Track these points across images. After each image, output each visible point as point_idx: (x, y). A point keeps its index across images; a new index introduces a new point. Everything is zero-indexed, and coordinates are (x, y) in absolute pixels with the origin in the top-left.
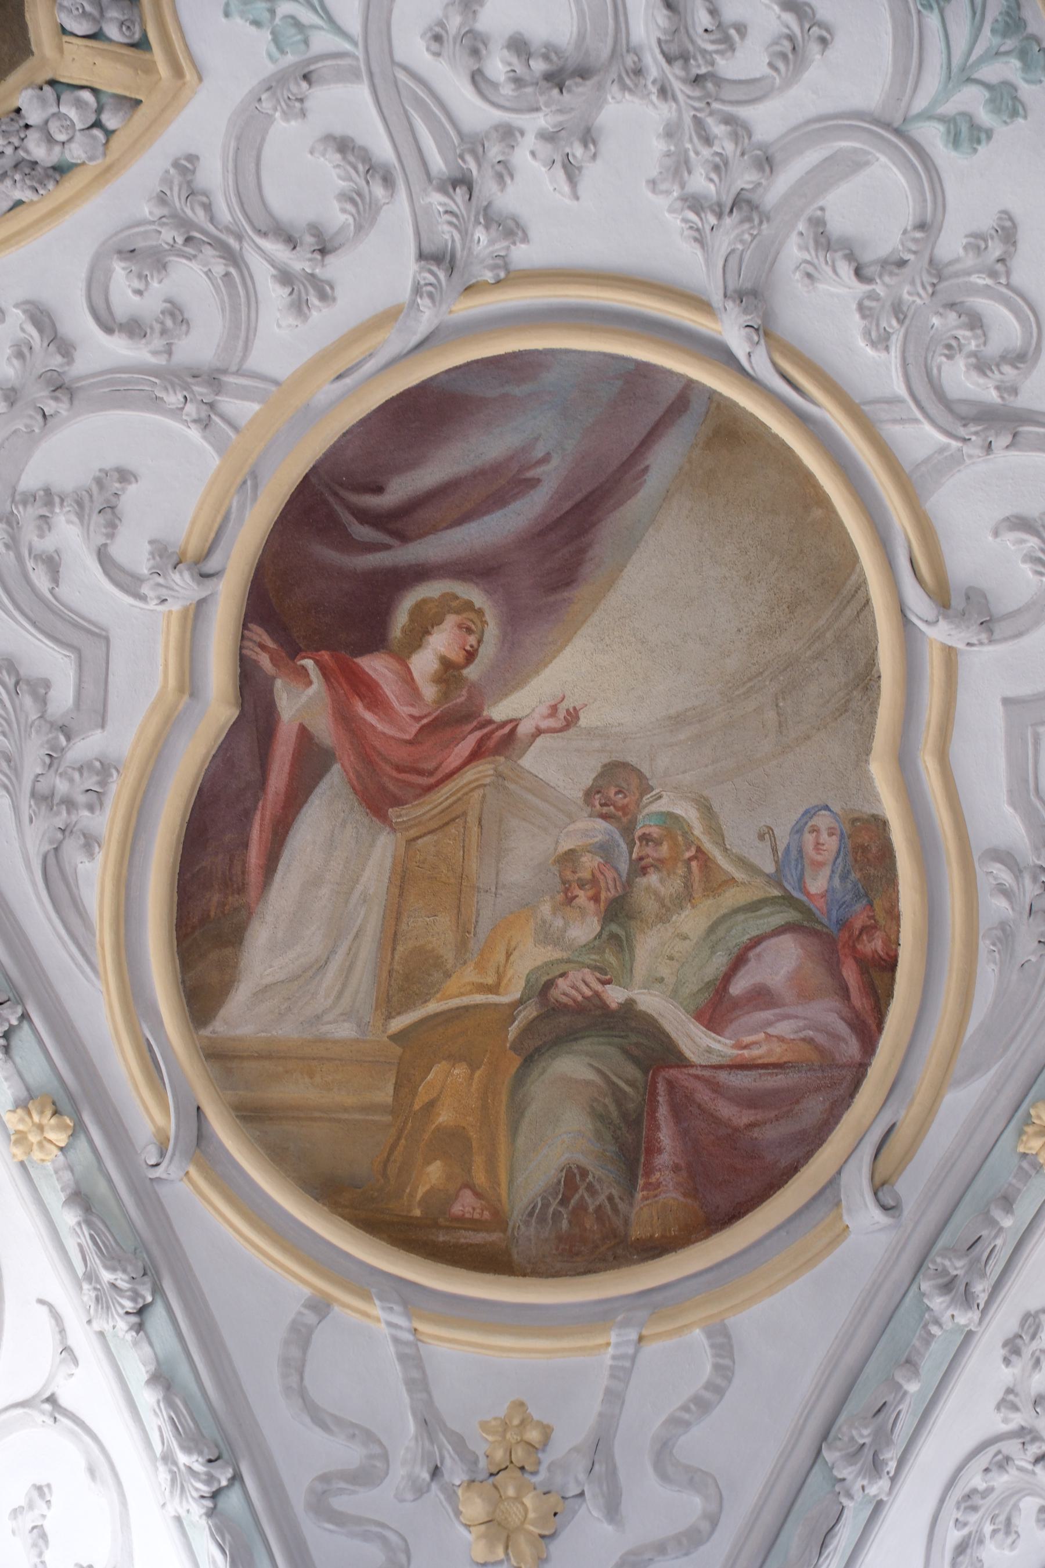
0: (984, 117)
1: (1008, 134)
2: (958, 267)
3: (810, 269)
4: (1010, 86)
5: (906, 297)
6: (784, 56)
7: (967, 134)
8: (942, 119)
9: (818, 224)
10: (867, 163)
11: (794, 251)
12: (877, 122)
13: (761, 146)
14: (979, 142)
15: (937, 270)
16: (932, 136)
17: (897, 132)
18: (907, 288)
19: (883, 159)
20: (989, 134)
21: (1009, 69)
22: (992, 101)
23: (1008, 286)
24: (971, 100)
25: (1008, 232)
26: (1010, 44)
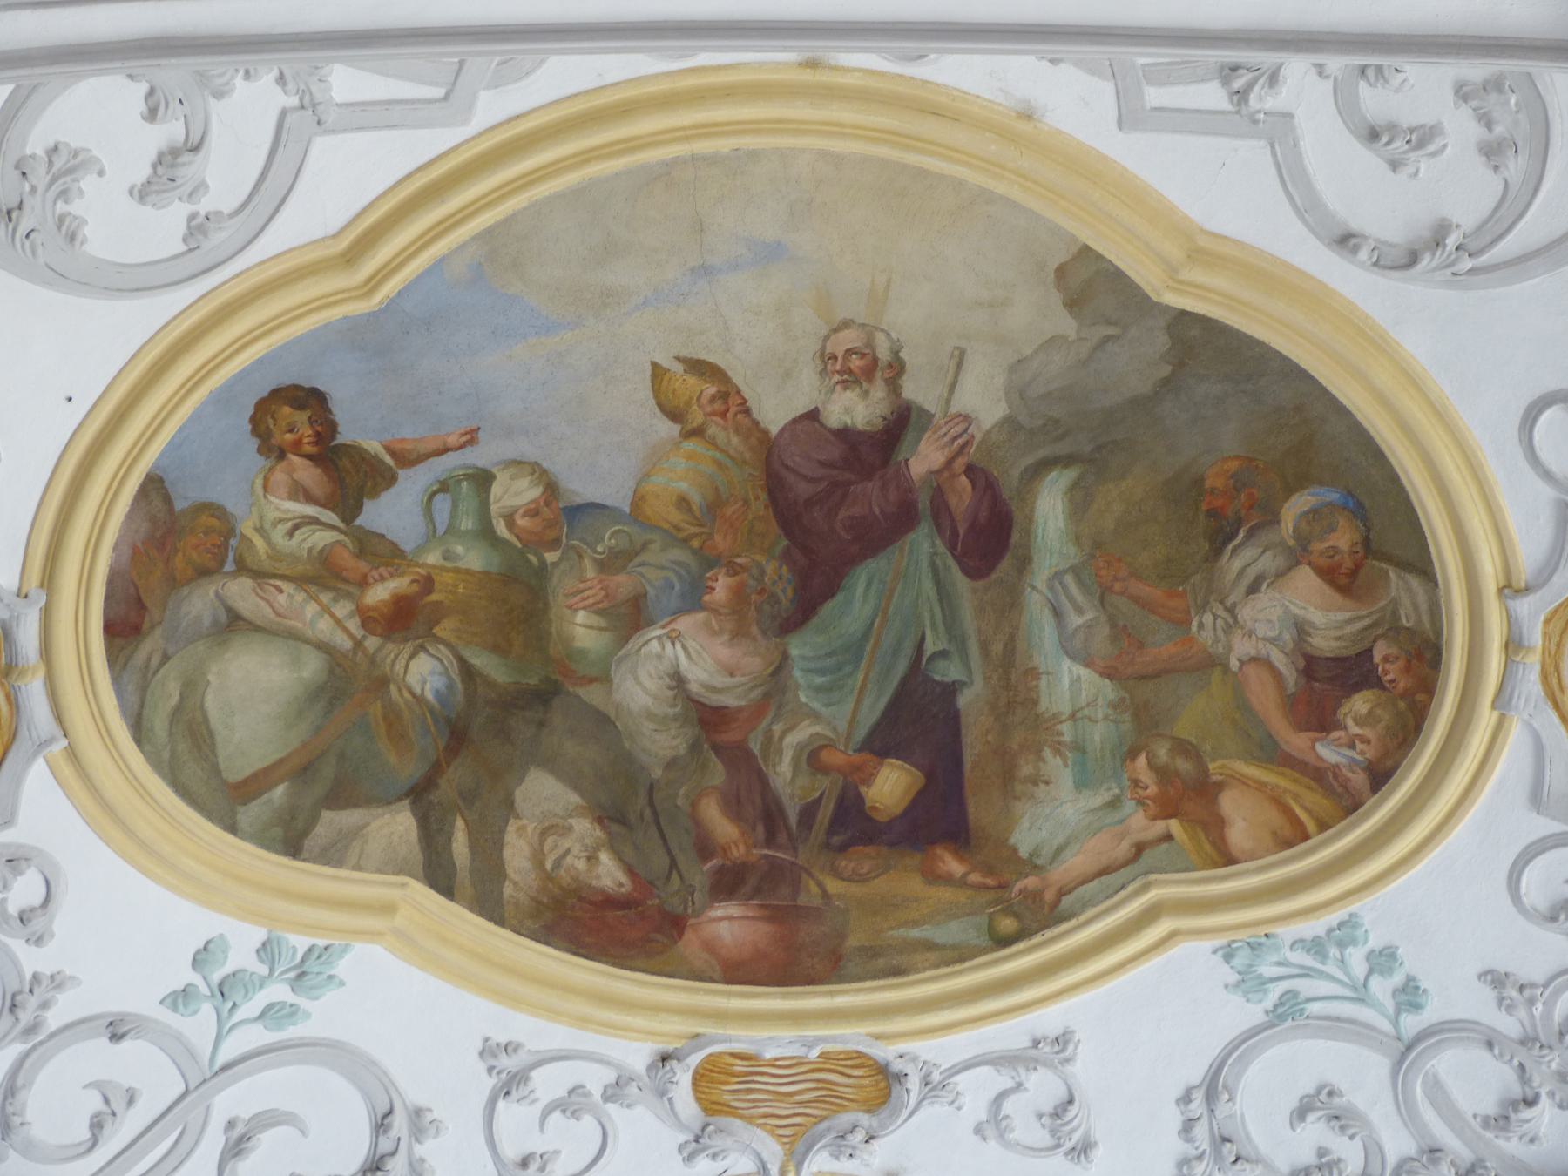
0: (1398, 979)
1: (1411, 962)
2: (1526, 1023)
3: (1527, 1139)
4: (1370, 955)
5: (1554, 1066)
6: (1342, 1128)
7: (1410, 995)
8: (1398, 1012)
9: (1486, 1122)
10: (1435, 1076)
11: (1512, 1146)
12: (1400, 1062)
13: (1422, 1152)
14: (1417, 988)
15: (1526, 1041)
16: (1411, 1024)
17: (1409, 1048)
18: (1544, 1067)
19: (1434, 1062)
20: (1410, 979)
21: (1356, 959)
22: (1382, 973)
23: (1545, 986)
24: (1381, 988)
25: (1496, 979)
26: (1333, 951)
